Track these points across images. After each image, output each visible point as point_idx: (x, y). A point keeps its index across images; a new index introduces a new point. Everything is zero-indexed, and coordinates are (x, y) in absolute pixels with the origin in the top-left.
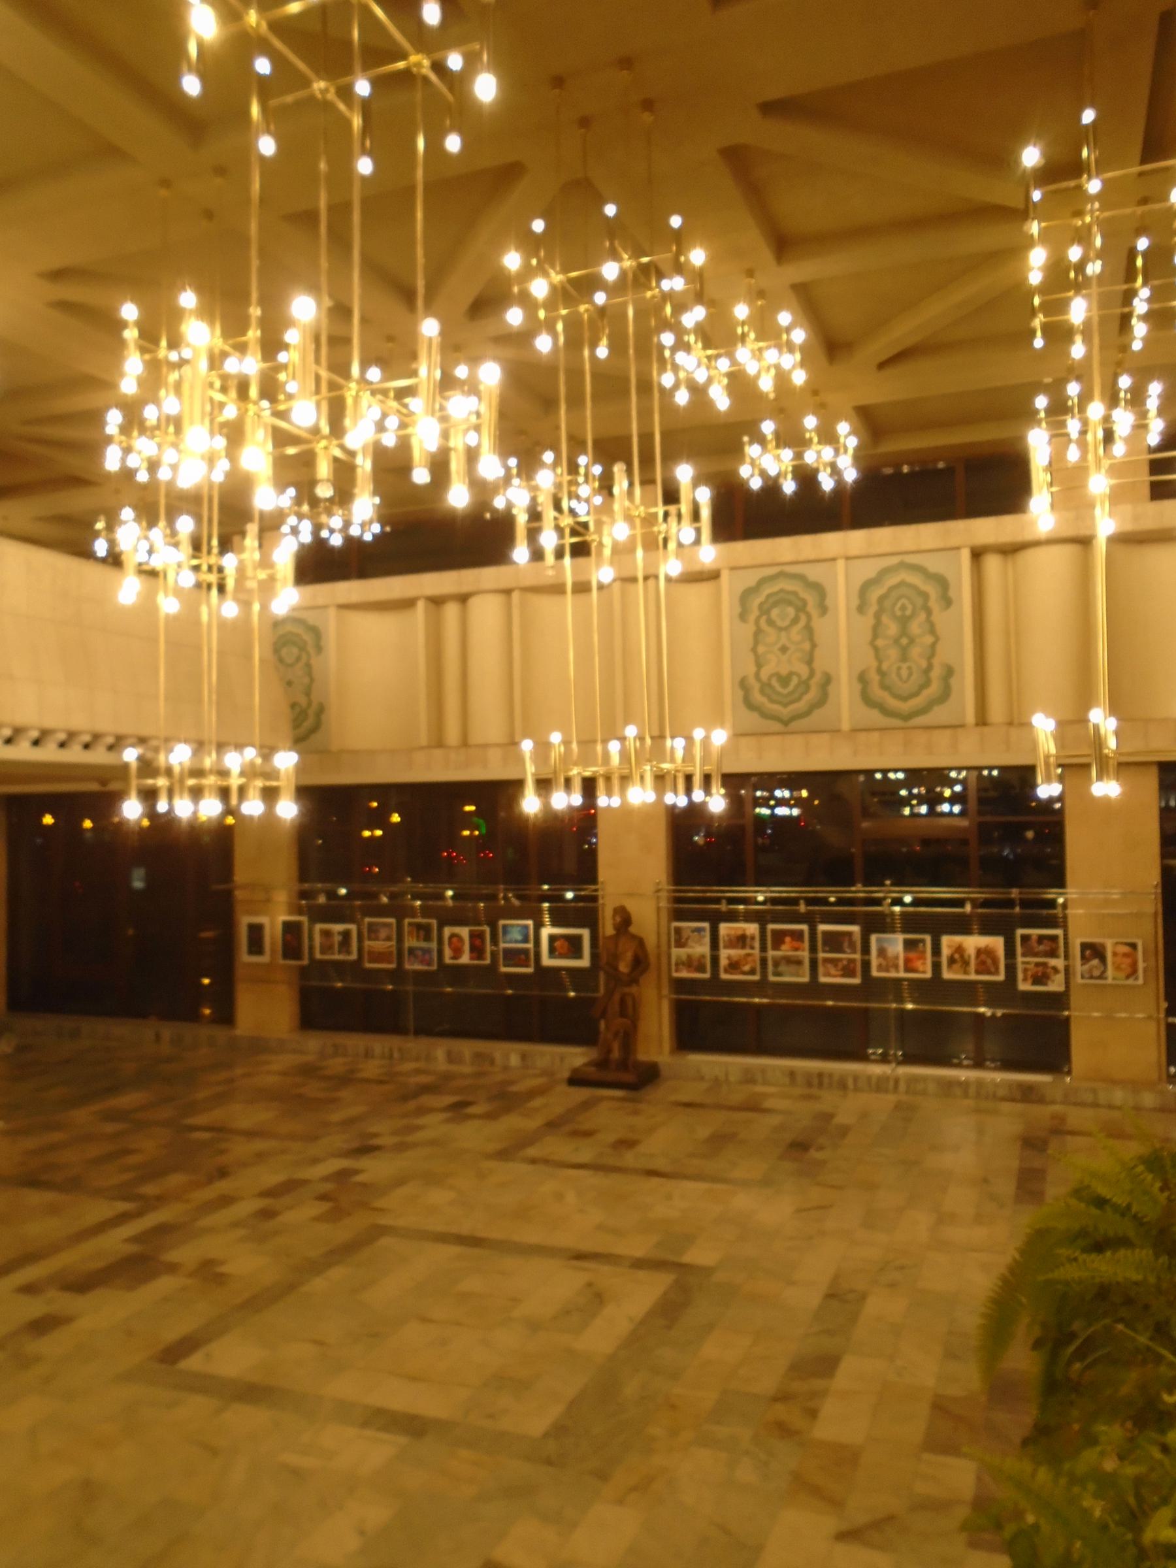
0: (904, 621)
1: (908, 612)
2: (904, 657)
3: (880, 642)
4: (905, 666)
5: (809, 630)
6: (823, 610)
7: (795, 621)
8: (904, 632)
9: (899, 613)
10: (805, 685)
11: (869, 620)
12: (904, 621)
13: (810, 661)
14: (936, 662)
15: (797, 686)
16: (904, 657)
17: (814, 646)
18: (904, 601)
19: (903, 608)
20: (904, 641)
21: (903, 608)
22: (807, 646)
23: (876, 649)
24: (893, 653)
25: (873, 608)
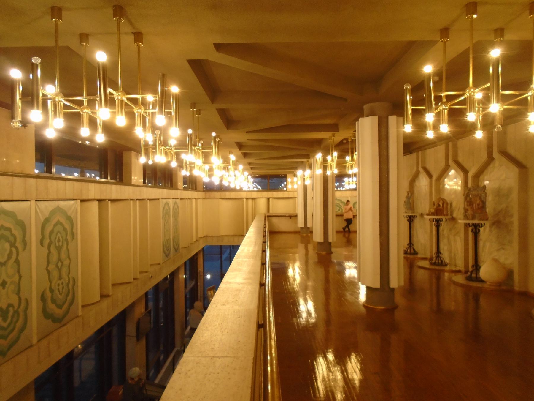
0: (59, 249)
1: (61, 244)
2: (60, 278)
3: (52, 267)
4: (60, 282)
5: (17, 261)
6: (25, 243)
7: (10, 256)
8: (59, 260)
9: (57, 245)
10: (16, 312)
11: (45, 250)
12: (59, 249)
13: (18, 293)
14: (70, 276)
15: (13, 317)
16: (60, 278)
17: (20, 277)
18: (59, 235)
19: (59, 241)
20: (60, 264)
21: (59, 241)
22: (17, 278)
23: (48, 272)
24: (55, 274)
25: (47, 242)
